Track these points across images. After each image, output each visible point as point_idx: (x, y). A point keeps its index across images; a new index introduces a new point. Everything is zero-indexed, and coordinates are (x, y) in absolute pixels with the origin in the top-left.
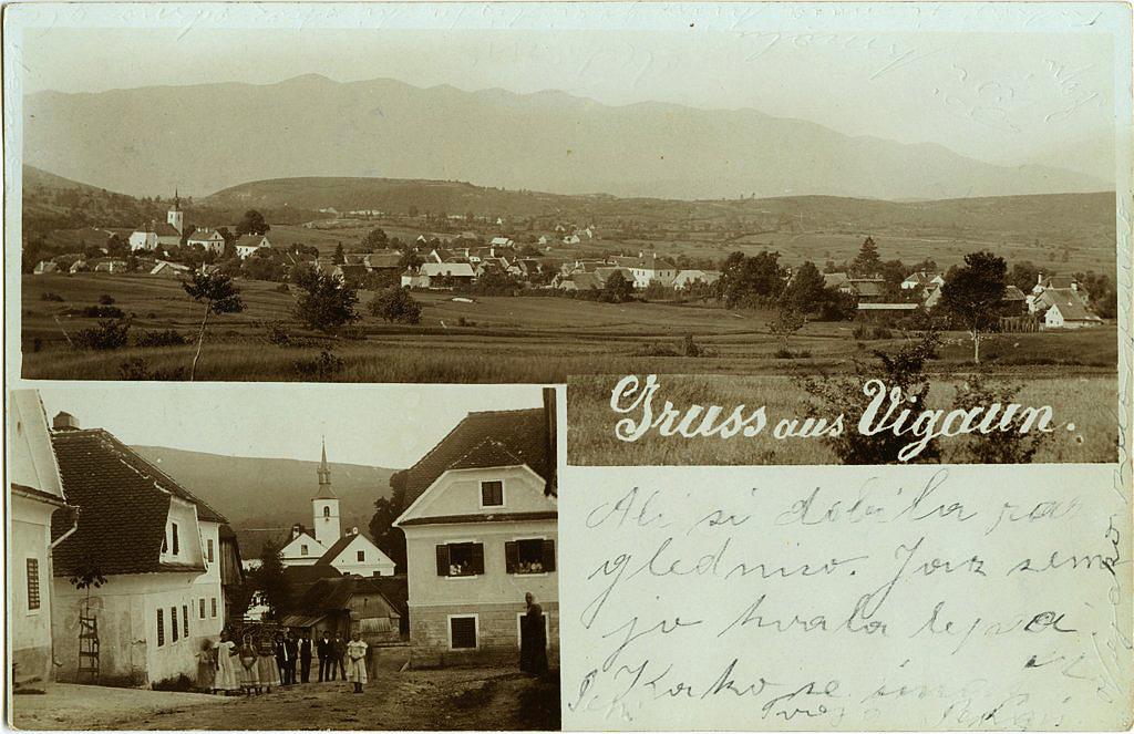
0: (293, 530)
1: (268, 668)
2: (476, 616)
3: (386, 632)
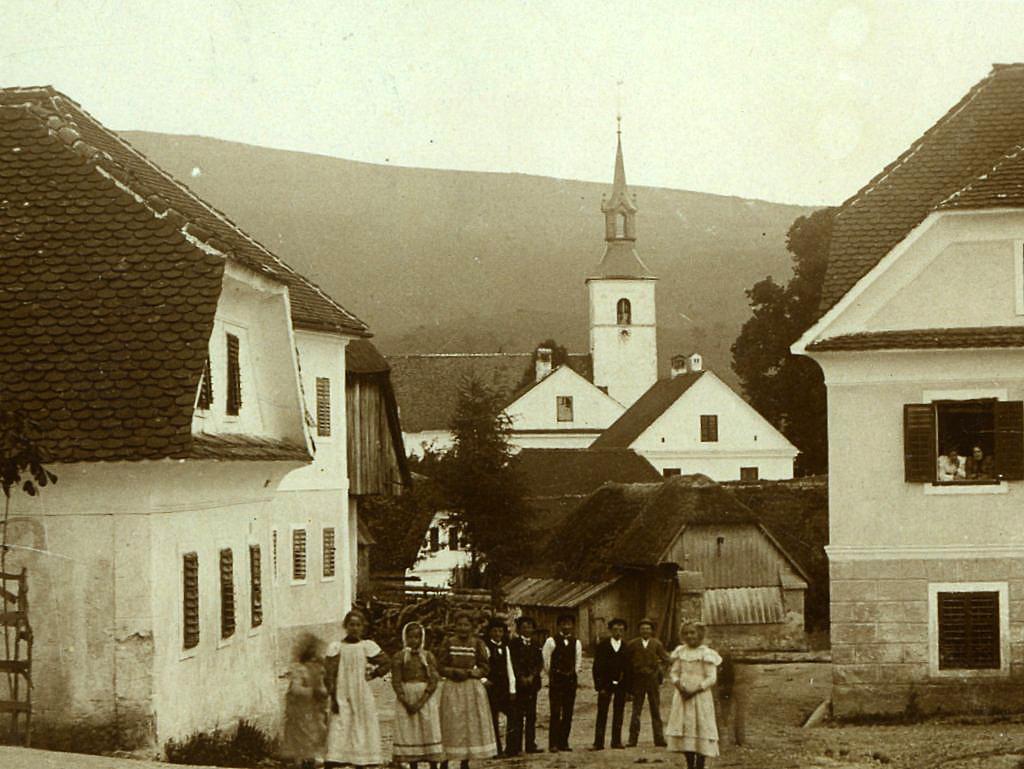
0: (535, 357)
1: (466, 712)
2: (1002, 589)
3: (768, 624)
